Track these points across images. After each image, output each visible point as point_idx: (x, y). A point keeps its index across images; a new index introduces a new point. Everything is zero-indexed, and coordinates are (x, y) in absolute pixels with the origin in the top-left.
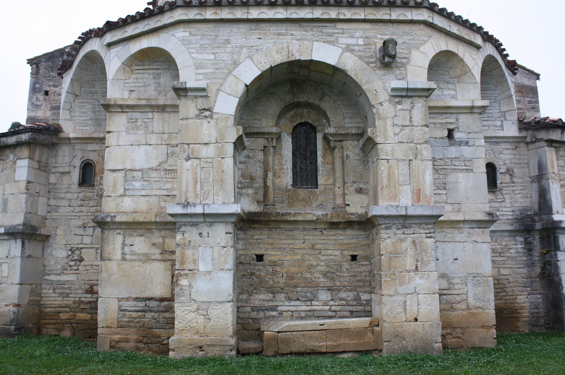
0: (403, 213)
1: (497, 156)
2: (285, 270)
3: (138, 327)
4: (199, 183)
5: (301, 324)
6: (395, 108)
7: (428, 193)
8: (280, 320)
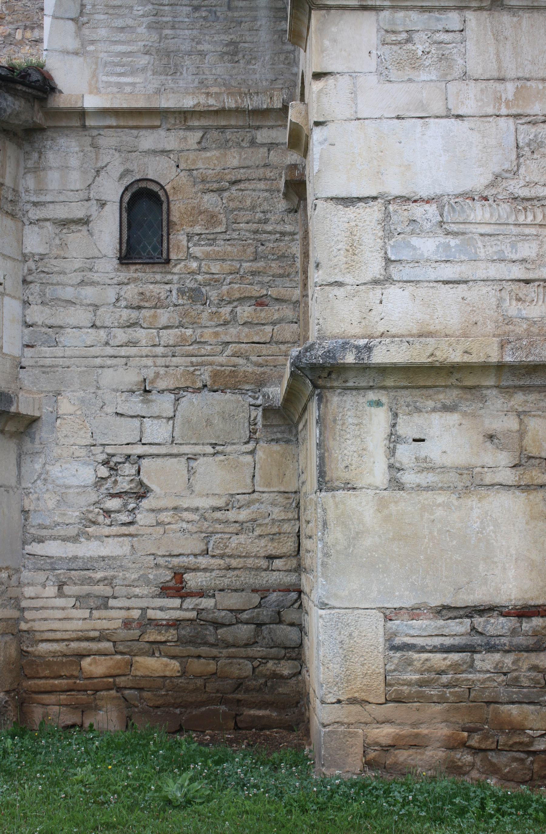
3: (452, 699)
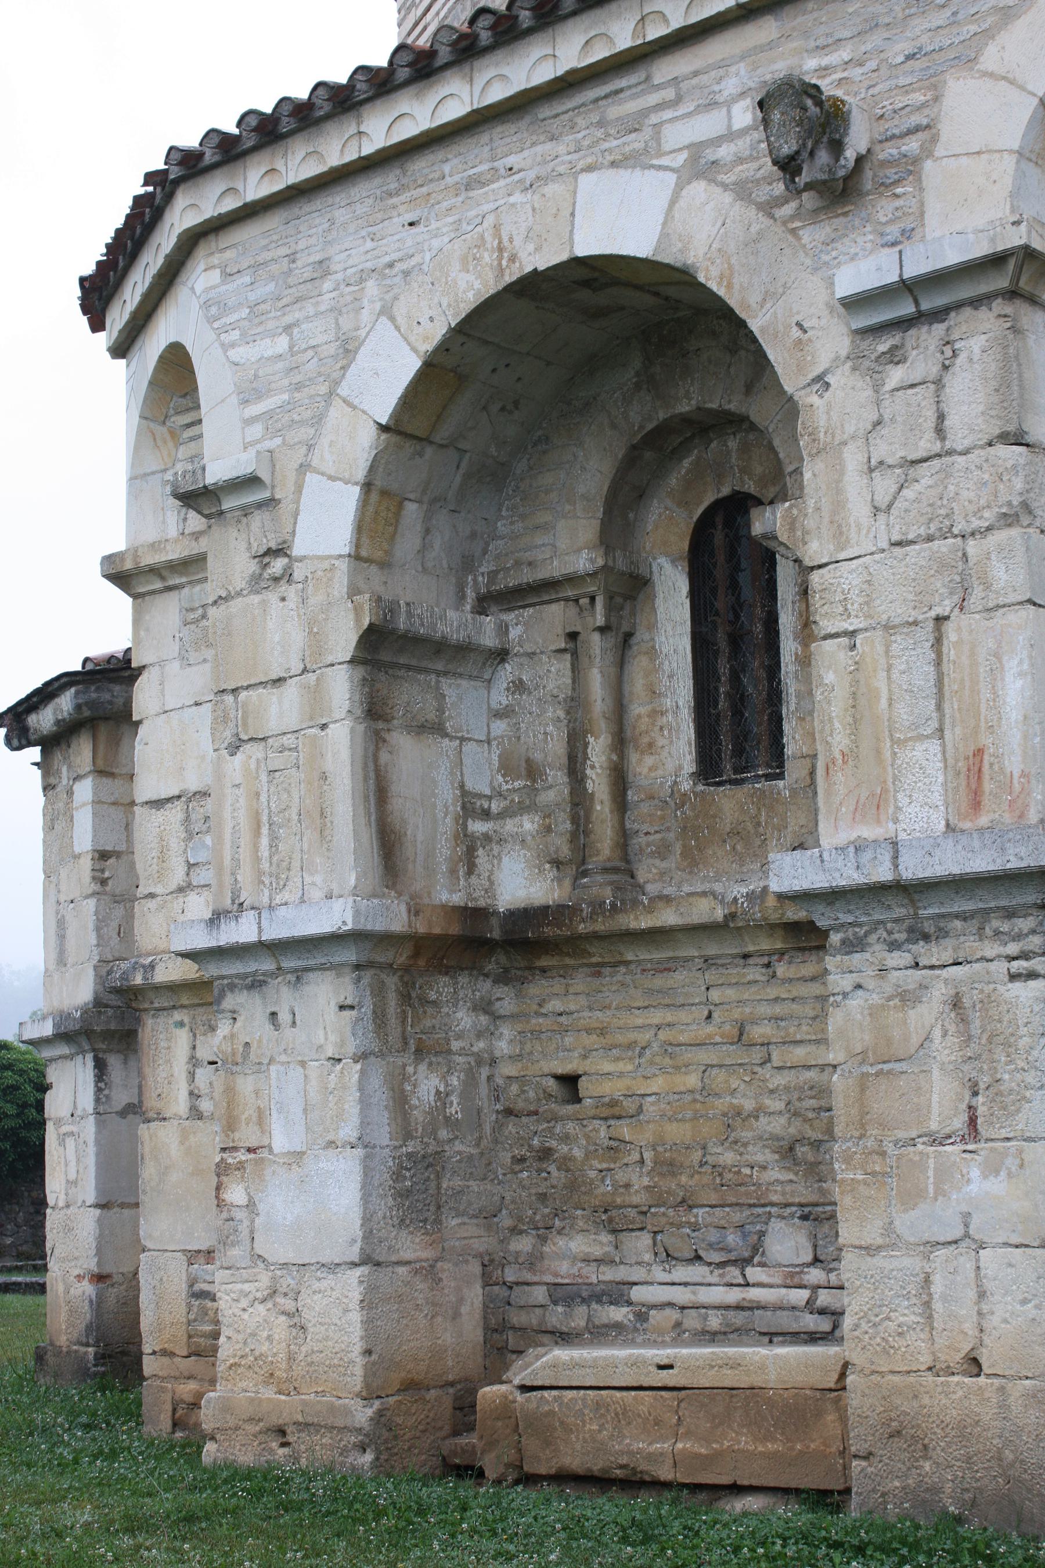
0: (883, 873)
2: (646, 1136)
4: (265, 830)
5: (595, 1360)
6: (877, 388)
7: (1014, 764)
8: (639, 1340)
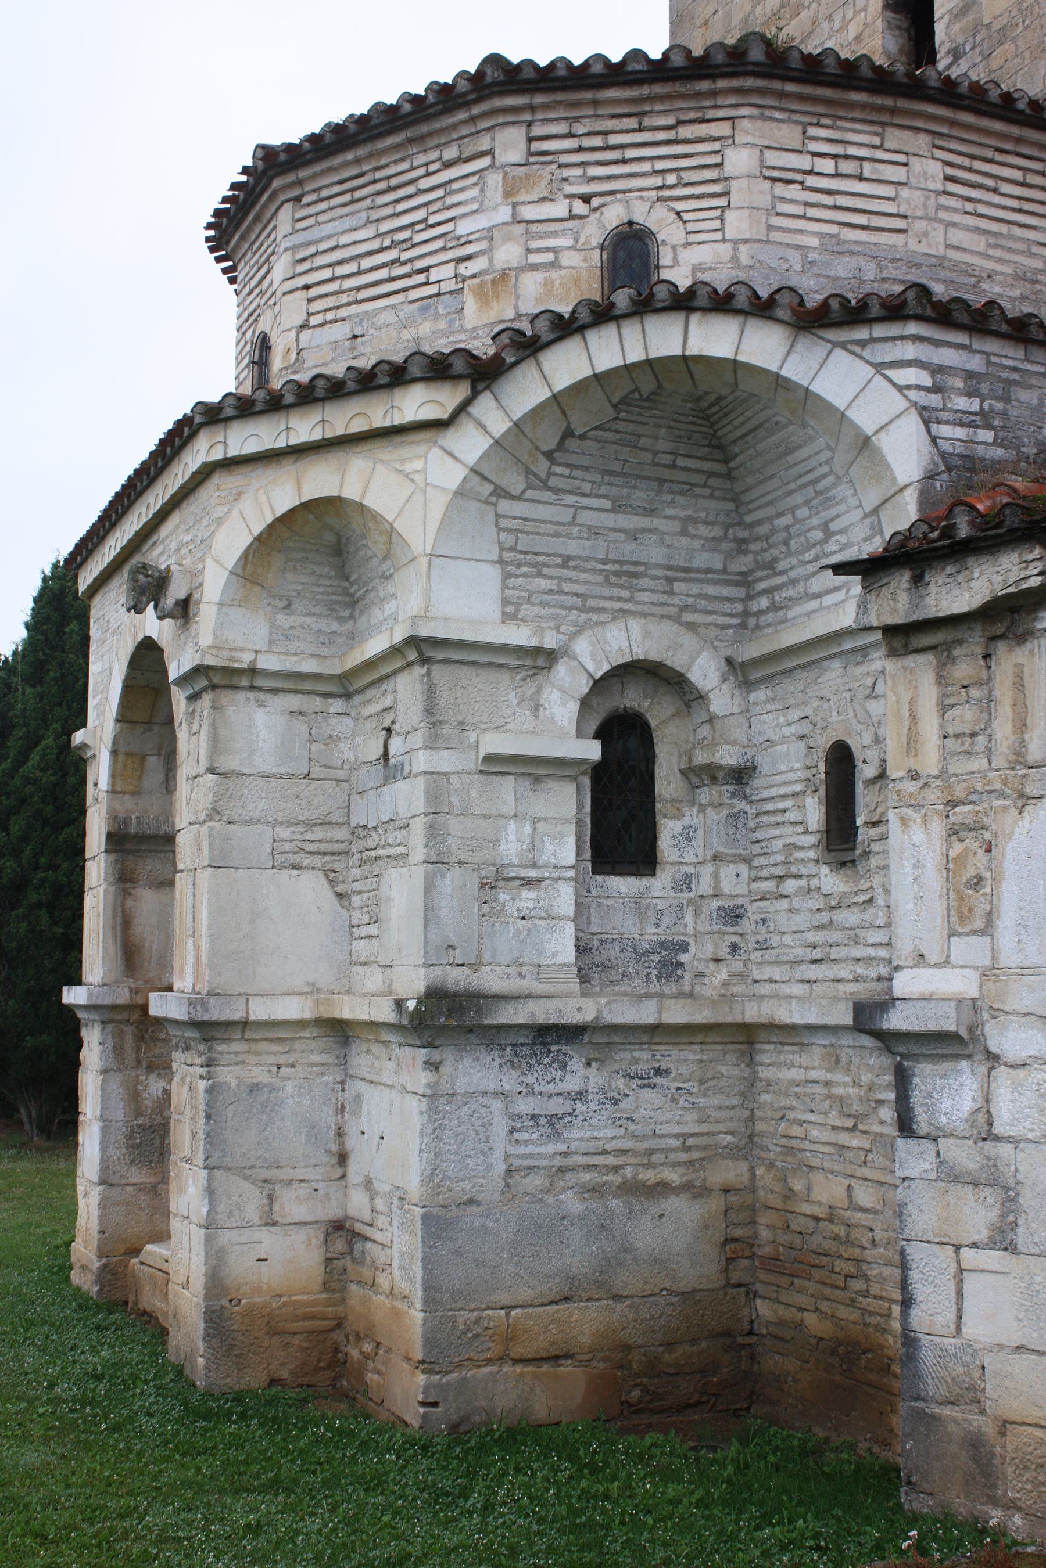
1: (859, 709)
